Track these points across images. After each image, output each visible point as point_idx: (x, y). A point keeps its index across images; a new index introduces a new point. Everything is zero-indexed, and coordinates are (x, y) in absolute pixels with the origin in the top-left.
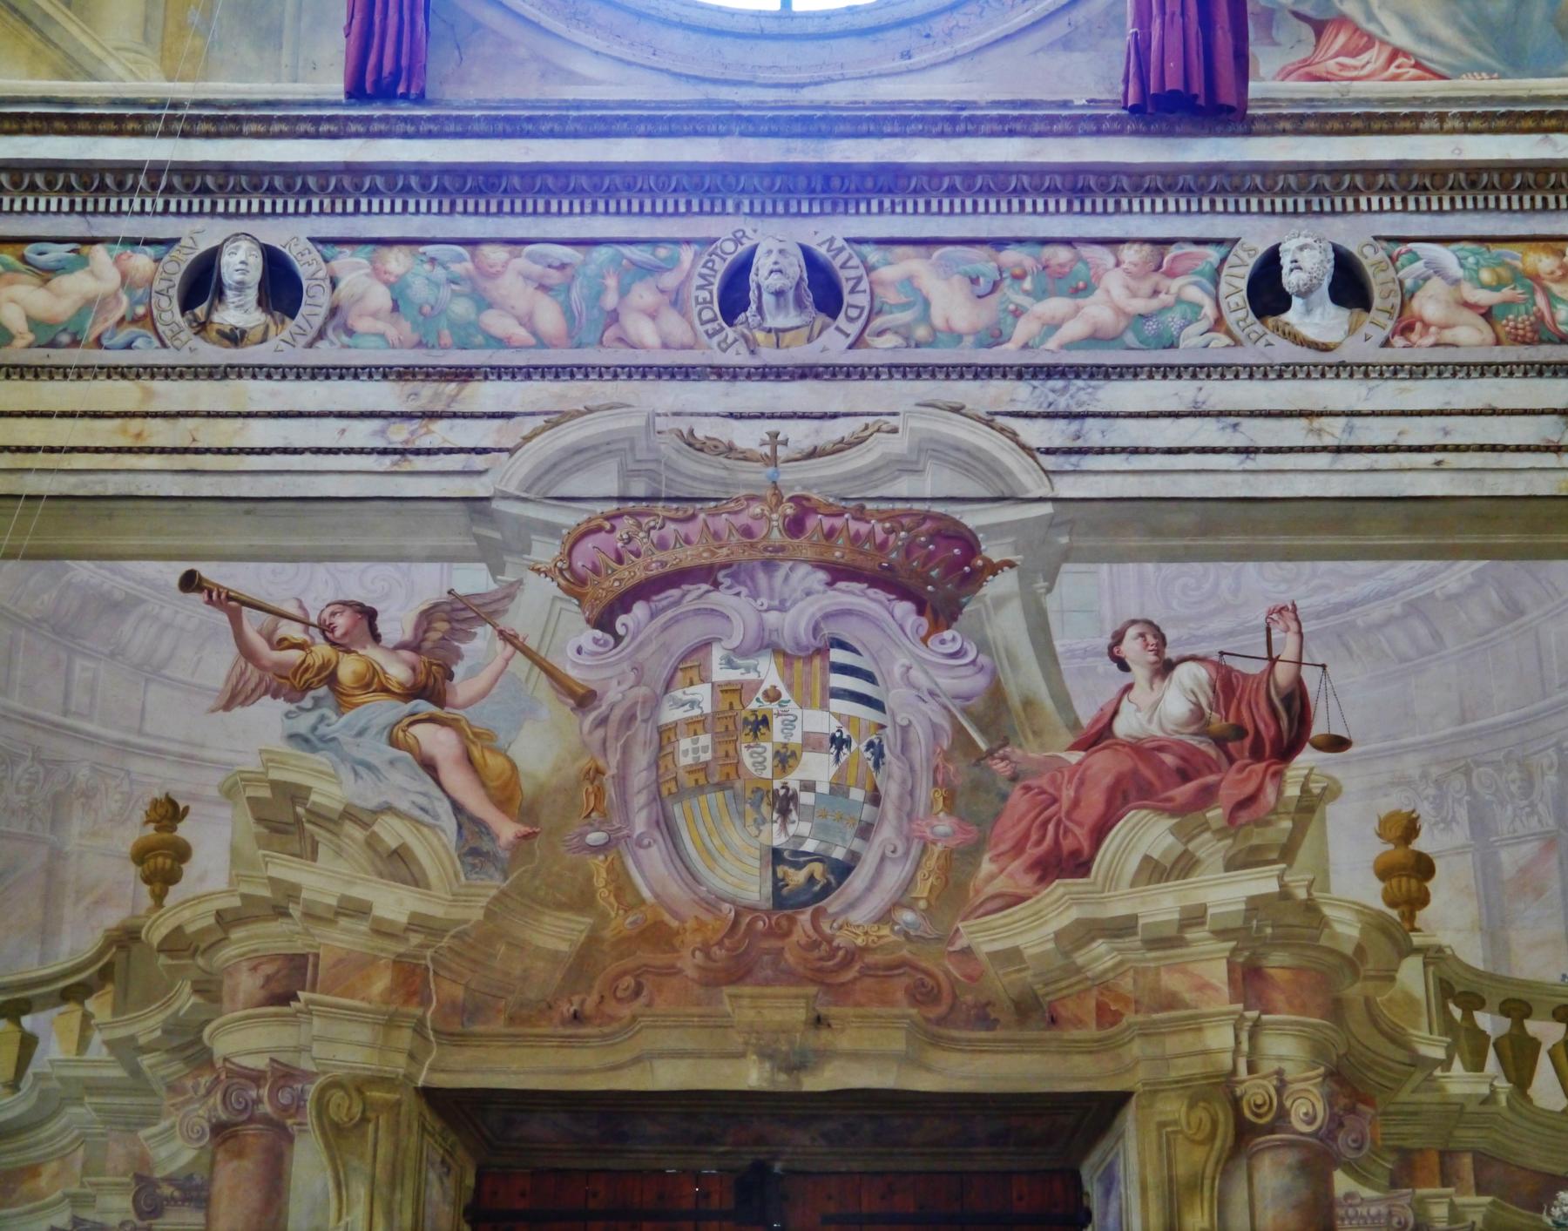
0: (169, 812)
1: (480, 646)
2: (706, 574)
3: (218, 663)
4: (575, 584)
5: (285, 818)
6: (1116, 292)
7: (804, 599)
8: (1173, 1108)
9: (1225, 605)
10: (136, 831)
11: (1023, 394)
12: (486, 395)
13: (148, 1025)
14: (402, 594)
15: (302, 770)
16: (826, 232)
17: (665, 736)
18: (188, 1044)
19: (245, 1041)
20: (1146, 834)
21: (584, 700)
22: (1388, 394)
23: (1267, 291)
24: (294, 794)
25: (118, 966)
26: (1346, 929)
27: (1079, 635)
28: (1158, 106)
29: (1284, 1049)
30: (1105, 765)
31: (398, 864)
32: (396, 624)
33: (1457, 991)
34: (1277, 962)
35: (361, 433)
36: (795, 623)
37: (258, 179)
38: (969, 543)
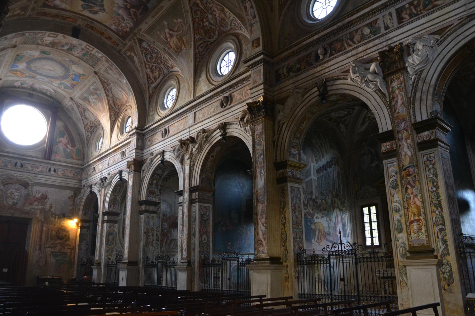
2: (11, 183)
6: (40, 169)
7: (17, 186)
9: (43, 190)
11: (34, 175)
16: (22, 162)
17: (7, 194)
20: (37, 203)
26: (47, 210)
27: (34, 191)
28: (45, 158)
29: (42, 216)
36: (16, 187)
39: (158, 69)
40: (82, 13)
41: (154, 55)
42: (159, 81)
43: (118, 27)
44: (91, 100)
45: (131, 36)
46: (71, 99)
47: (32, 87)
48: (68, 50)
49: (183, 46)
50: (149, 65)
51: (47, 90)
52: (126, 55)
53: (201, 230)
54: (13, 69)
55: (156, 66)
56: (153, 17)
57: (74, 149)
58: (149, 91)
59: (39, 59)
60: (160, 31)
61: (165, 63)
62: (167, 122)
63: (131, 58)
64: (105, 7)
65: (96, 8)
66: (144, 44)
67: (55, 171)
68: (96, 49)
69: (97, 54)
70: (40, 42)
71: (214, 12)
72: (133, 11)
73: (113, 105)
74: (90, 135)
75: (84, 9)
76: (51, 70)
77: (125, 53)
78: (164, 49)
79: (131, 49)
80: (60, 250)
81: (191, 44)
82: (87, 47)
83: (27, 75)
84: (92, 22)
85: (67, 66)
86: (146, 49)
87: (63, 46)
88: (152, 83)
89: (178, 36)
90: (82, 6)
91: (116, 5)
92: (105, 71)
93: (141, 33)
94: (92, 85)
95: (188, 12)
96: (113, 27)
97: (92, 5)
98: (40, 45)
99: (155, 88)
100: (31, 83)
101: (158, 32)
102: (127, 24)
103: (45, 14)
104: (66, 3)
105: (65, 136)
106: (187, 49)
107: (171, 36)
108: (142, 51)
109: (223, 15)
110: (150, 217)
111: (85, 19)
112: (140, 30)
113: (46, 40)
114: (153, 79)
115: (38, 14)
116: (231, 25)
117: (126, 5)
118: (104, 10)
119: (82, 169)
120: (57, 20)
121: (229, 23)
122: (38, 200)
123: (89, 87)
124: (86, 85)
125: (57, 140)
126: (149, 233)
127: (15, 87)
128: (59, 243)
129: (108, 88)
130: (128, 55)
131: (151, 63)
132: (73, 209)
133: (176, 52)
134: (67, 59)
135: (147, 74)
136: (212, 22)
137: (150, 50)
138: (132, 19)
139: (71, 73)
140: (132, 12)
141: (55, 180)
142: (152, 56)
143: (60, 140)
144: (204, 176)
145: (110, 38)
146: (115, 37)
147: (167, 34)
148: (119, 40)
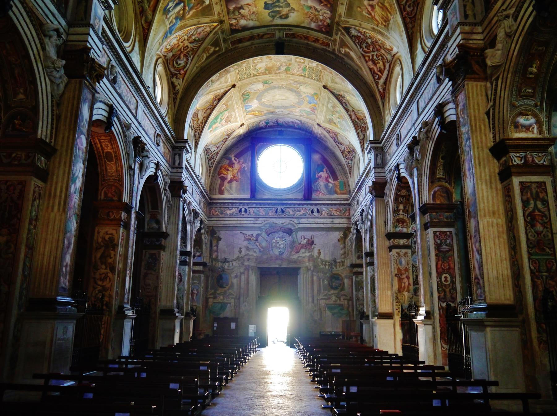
0: (240, 248)
1: (260, 237)
2: (274, 232)
3: (243, 238)
4: (266, 232)
5: (248, 249)
6: (302, 212)
7: (281, 234)
8: (304, 268)
10: (238, 250)
11: (296, 219)
12: (260, 219)
13: (240, 262)
14: (255, 233)
15: (249, 246)
16: (283, 207)
17: (272, 244)
18: (243, 264)
19: (246, 263)
20: (303, 250)
21: (267, 241)
22: (320, 220)
23: (312, 212)
24: (248, 247)
25: (238, 259)
26: (315, 257)
29: (311, 265)
30: (300, 246)
31: (255, 252)
32: (254, 236)
33: (322, 261)
34: (311, 259)
35: (252, 222)
36: (280, 236)
37: (244, 203)
38: (292, 230)
39: (380, 58)
41: (369, 41)
42: (386, 72)
43: (318, 22)
44: (335, 121)
45: (335, 28)
46: (318, 125)
47: (277, 124)
48: (287, 70)
49: (389, 15)
50: (369, 57)
51: (292, 122)
52: (342, 53)
53: (439, 266)
54: (248, 110)
55: (377, 55)
57: (337, 183)
58: (379, 90)
59: (266, 91)
60: (360, 8)
61: (382, 46)
62: (397, 124)
63: (347, 55)
66: (353, 32)
67: (318, 211)
68: (307, 60)
69: (310, 64)
70: (256, 73)
73: (356, 120)
74: (350, 162)
77: (340, 52)
78: (373, 28)
79: (343, 44)
80: (336, 301)
81: (395, 8)
84: (290, 30)
86: (358, 37)
88: (379, 78)
89: (380, 4)
90: (269, 14)
93: (343, 19)
94: (328, 102)
96: (313, 25)
97: (278, 9)
98: (257, 75)
99: (385, 83)
100: (274, 120)
101: (359, 9)
102: (325, 15)
103: (240, 41)
104: (252, 20)
105: (325, 170)
106: (393, 18)
107: (372, 6)
108: (354, 42)
110: (402, 254)
111: (281, 29)
114: (379, 73)
115: (233, 43)
119: (350, 204)
120: (255, 42)
122: (304, 246)
123: (327, 106)
124: (323, 104)
125: (317, 177)
126: (401, 275)
127: (262, 128)
128: (333, 294)
131: (369, 52)
132: (345, 253)
133: (385, 26)
135: (370, 69)
137: (362, 37)
138: (325, 5)
139: (303, 96)
141: (319, 222)
142: (367, 43)
143: (319, 175)
144: (436, 189)
145: (317, 40)
146: (321, 36)
147: (368, 7)
148: (326, 38)
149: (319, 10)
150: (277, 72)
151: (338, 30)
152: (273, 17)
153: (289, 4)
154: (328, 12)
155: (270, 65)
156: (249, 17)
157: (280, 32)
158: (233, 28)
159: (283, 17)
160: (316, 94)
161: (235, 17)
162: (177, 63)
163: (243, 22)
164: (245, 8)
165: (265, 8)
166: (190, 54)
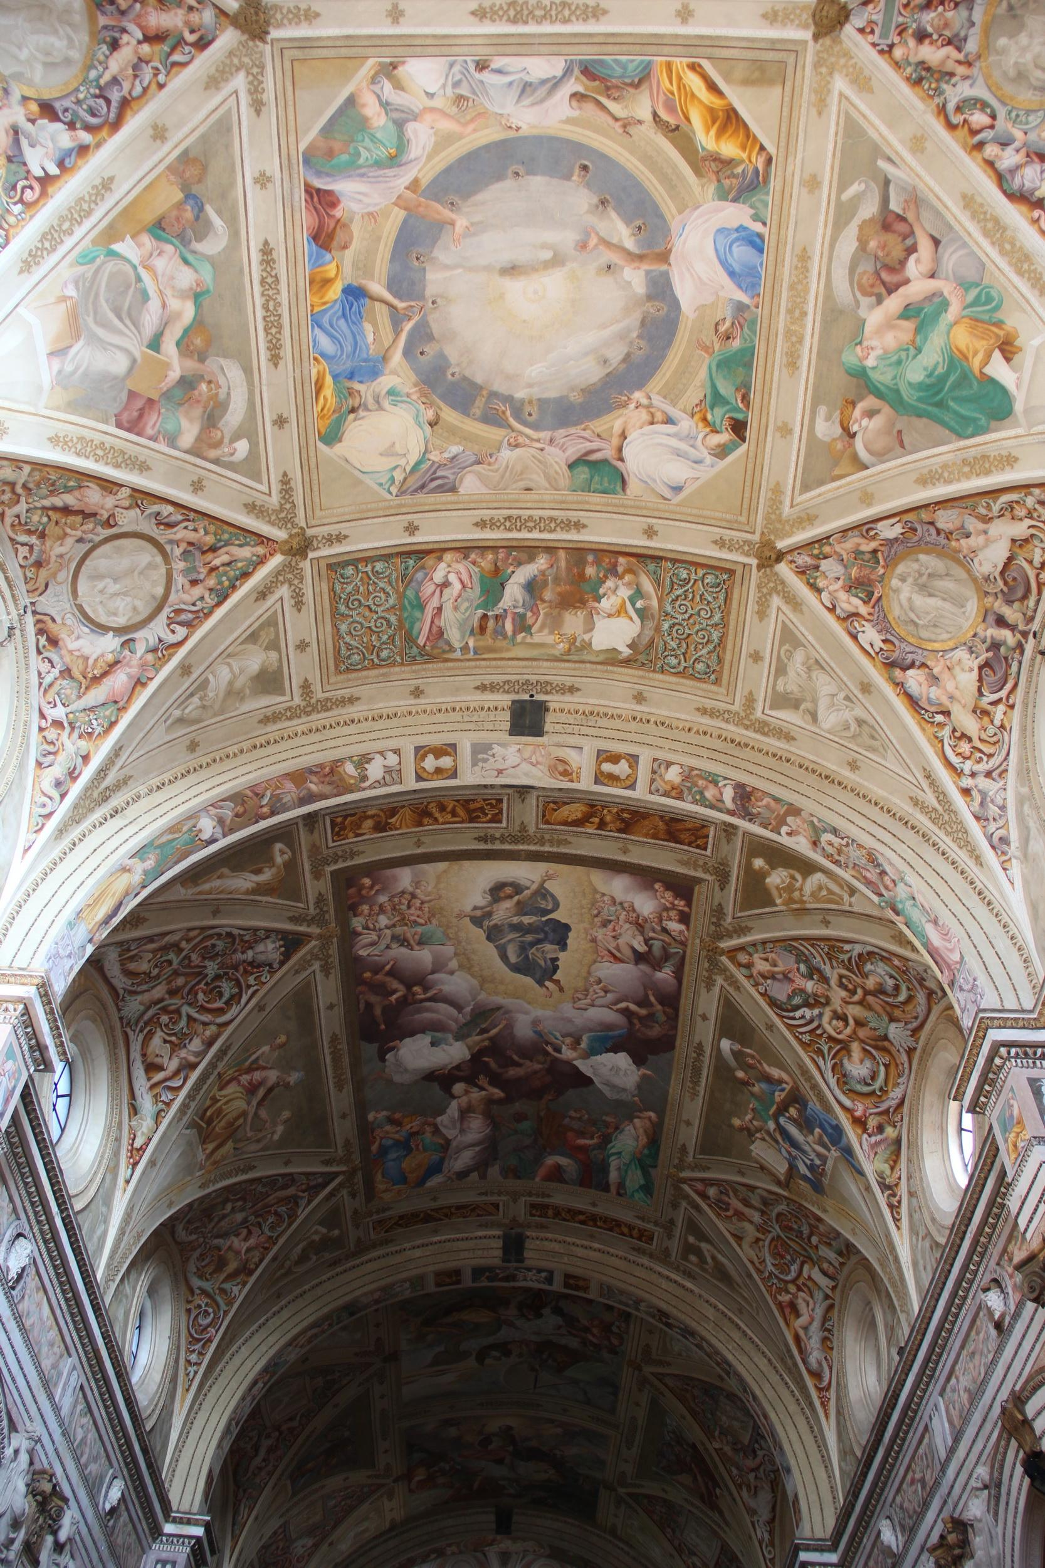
39: (155, 972)
40: (542, 867)
45: (331, 915)
56: (334, 1039)
64: (479, 934)
65: (504, 911)
68: (410, 783)
71: (245, 1232)
72: (395, 991)
73: (69, 499)
75: (542, 892)
76: (512, 270)
82: (446, 762)
83: (642, 106)
84: (484, 839)
85: (450, 416)
87: (532, 587)
91: (453, 964)
92: (271, 622)
93: (316, 966)
95: (286, 1164)
96: (405, 877)
101: (282, 1039)
102: (374, 937)
109: (232, 1266)
111: (516, 840)
112: (326, 970)
113: (621, 611)
116: (204, 1292)
117: (426, 989)
118: (477, 921)
121: (207, 1285)
129: (180, 533)
130: (278, 846)
131: (193, 949)
134: (470, 485)
136: (222, 1223)
137: (239, 956)
138: (377, 969)
139: (397, 357)
140: (395, 984)
147: (265, 1073)
148: (353, 855)
149: (394, 946)
150: (542, 562)
151: (319, 920)
152: (542, 892)
153: (489, 938)
154: (363, 953)
155: (573, 621)
156: (622, 917)
157: (523, 827)
158: (680, 904)
159: (508, 890)
160: (332, 436)
161: (667, 939)
162: (897, 988)
163: (646, 905)
164: (628, 953)
165: (567, 928)
166: (846, 957)
